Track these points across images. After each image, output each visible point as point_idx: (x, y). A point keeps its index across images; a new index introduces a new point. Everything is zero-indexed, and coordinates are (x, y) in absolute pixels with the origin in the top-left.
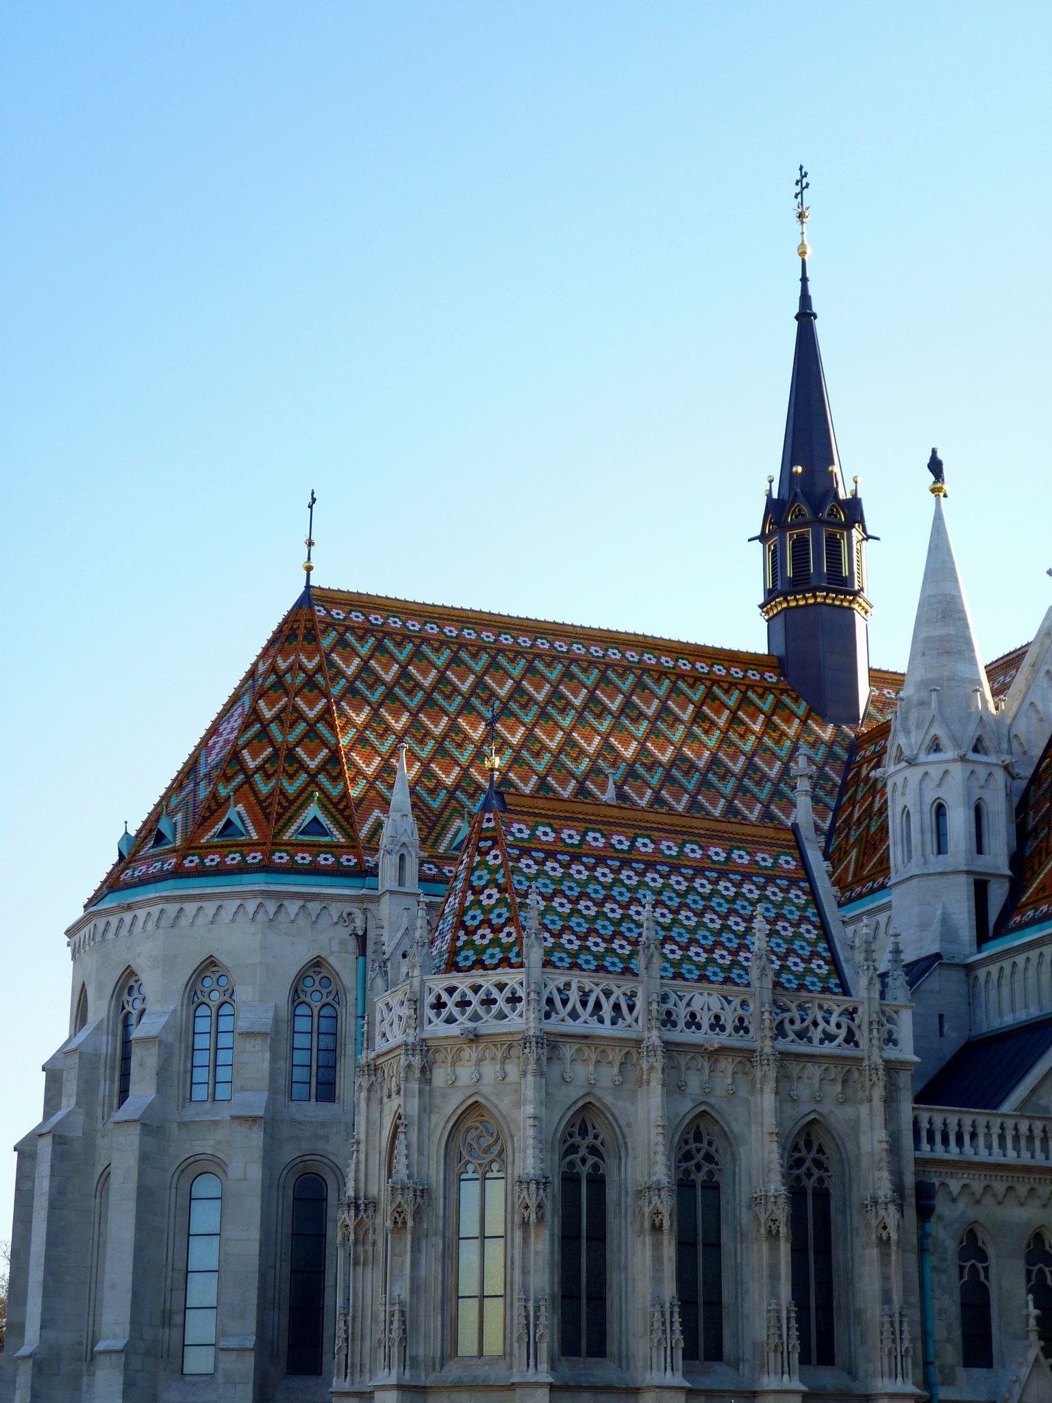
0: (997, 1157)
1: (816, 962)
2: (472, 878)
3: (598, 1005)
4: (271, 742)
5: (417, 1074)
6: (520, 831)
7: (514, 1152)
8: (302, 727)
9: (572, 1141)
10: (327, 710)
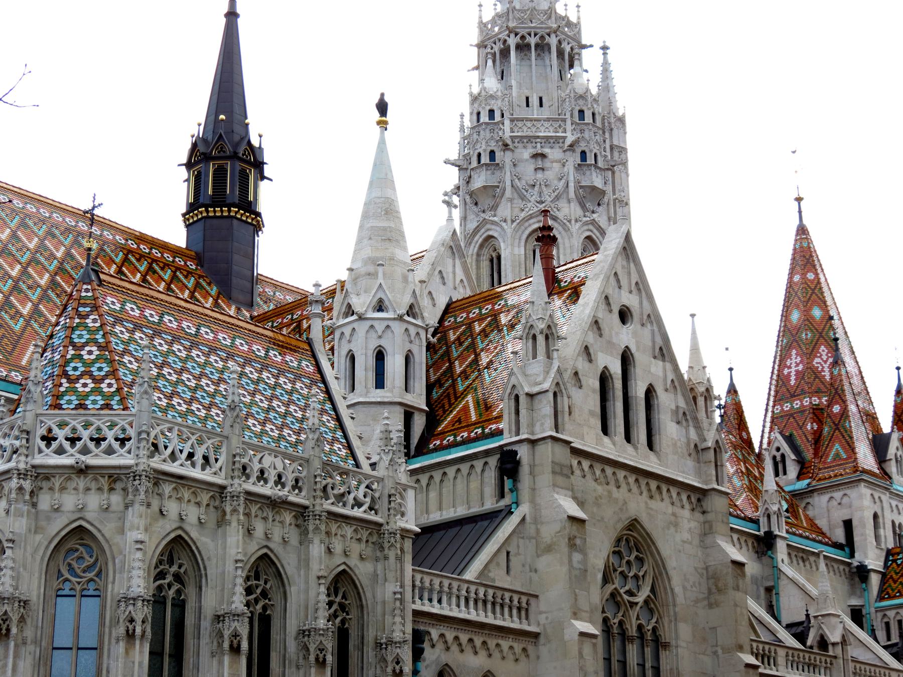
0: (463, 615)
1: (337, 446)
2: (73, 336)
3: (191, 456)
6: (113, 303)
7: (114, 572)
9: (162, 567)
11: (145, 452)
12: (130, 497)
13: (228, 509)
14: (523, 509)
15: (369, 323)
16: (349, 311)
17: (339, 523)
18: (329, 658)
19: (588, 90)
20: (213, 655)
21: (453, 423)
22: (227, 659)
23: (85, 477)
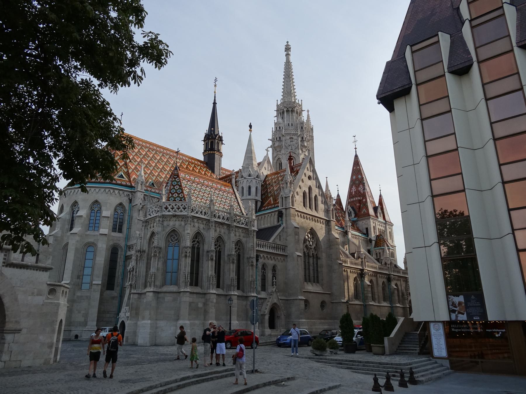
3: (201, 212)
12: (186, 222)
13: (210, 225)
14: (284, 225)
15: (247, 180)
16: (242, 177)
18: (235, 261)
19: (304, 121)
20: (207, 261)
21: (267, 204)
22: (210, 262)
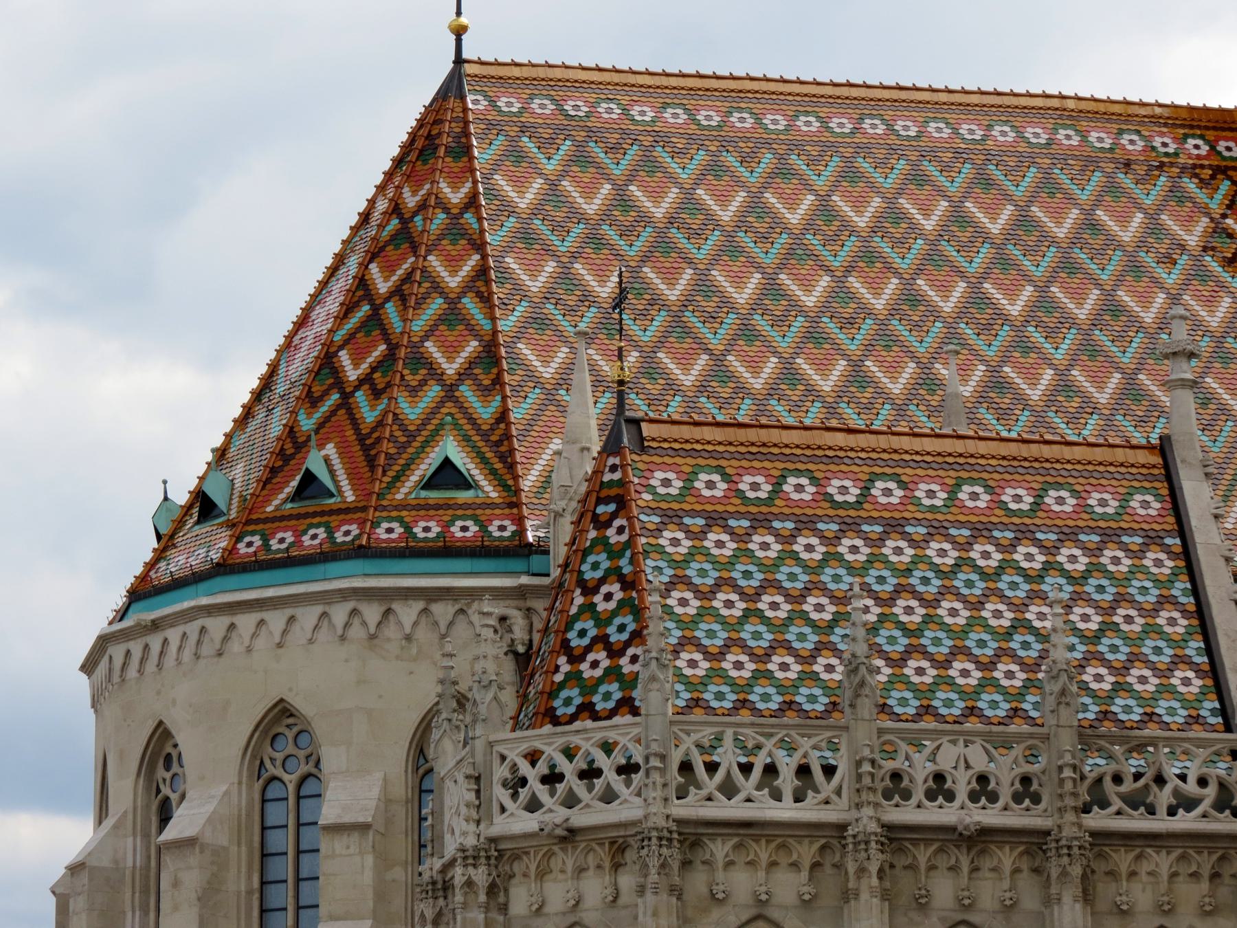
4: (386, 335)
5: (482, 898)
8: (436, 305)
10: (482, 272)
11: (654, 795)
17: (1138, 850)
23: (575, 848)
